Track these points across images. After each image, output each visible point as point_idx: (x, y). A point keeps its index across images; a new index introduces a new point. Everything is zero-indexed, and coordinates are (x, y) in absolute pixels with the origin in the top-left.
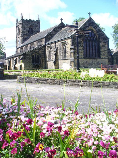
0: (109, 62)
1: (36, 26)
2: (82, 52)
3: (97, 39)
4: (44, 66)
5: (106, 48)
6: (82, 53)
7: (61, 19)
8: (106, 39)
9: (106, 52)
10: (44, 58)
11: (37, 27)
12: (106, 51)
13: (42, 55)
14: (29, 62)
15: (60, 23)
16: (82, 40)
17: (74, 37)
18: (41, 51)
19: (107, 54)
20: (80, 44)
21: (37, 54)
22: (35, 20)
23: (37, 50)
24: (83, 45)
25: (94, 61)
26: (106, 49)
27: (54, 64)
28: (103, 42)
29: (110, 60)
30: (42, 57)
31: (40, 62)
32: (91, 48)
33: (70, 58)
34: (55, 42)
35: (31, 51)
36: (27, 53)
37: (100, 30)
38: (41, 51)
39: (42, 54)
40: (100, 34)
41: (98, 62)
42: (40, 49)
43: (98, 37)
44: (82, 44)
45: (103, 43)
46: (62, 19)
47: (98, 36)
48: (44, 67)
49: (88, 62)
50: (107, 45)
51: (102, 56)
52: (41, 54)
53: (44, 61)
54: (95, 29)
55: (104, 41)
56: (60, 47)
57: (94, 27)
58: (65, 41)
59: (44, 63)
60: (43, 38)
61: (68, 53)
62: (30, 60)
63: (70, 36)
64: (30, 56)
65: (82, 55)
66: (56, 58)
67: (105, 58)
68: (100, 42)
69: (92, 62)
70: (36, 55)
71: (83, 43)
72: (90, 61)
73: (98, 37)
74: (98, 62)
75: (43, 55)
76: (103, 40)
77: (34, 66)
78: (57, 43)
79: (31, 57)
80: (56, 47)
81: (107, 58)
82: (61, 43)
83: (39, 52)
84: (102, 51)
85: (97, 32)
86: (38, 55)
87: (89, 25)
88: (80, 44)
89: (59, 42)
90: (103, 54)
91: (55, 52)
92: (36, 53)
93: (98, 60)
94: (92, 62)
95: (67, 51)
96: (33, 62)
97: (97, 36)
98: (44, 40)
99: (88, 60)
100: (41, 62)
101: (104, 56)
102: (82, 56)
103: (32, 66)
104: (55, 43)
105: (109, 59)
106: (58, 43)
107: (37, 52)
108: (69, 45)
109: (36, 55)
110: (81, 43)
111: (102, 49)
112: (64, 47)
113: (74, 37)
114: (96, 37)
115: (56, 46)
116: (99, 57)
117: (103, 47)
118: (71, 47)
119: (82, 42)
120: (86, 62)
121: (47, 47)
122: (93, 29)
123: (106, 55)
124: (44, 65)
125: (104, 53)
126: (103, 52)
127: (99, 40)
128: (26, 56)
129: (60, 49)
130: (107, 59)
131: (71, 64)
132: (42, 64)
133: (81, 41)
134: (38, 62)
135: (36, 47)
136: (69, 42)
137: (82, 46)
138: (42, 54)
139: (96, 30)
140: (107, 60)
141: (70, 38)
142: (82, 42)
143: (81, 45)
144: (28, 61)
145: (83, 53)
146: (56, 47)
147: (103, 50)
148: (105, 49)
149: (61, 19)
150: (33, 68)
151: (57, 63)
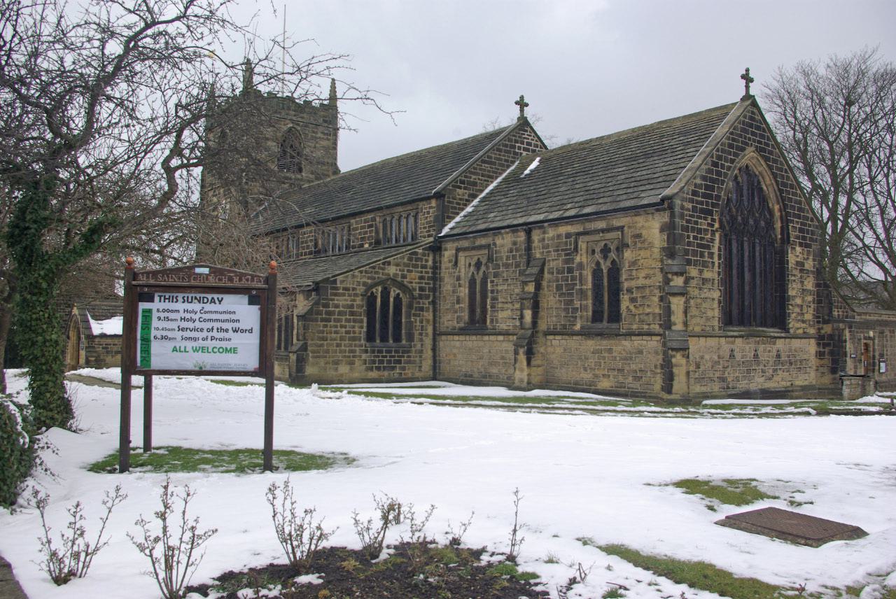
0: (820, 355)
1: (319, 135)
2: (716, 294)
3: (770, 224)
4: (430, 362)
5: (811, 276)
6: (716, 305)
7: (522, 104)
8: (810, 226)
9: (810, 298)
10: (429, 315)
11: (325, 143)
12: (810, 292)
13: (421, 297)
14: (347, 332)
15: (507, 118)
16: (717, 225)
17: (682, 207)
18: (415, 275)
19: (811, 311)
20: (708, 247)
21: (394, 292)
22: (316, 103)
23: (397, 265)
24: (719, 259)
25: (761, 347)
26: (810, 284)
27: (522, 358)
28: (801, 245)
29: (828, 345)
30: (422, 309)
31: (410, 338)
32: (747, 276)
33: (656, 328)
34: (528, 228)
35: (366, 272)
36: (342, 282)
37: (788, 178)
38: (415, 275)
39: (422, 289)
40: (790, 200)
41: (778, 356)
42: (410, 259)
43: (777, 214)
44: (715, 250)
45: (798, 249)
46: (527, 105)
47: (780, 210)
48: (427, 365)
49: (738, 356)
50: (814, 260)
51: (793, 324)
52: (415, 290)
53: (430, 329)
54: (770, 168)
55: (804, 238)
56: (567, 262)
57: (766, 159)
58: (616, 223)
59: (428, 342)
60: (428, 198)
61: (633, 300)
62: (355, 321)
63: (663, 200)
64: (359, 301)
65: (716, 314)
66: (535, 323)
67: (805, 336)
68: (786, 239)
69: (756, 356)
70: (386, 294)
71: (720, 243)
73: (777, 214)
74: (778, 356)
75: (427, 297)
77: (374, 362)
78: (536, 236)
79: (359, 306)
80: (529, 259)
81: (812, 331)
82: (579, 234)
83: (404, 277)
84: (794, 294)
85: (777, 182)
86: (398, 299)
87: (747, 144)
88: (708, 247)
89: (563, 230)
90: (797, 310)
91: (531, 288)
92: (386, 285)
93: (780, 344)
94: (756, 356)
95: (626, 285)
96: (370, 337)
97: (776, 207)
98: (429, 210)
99: (739, 341)
100: (416, 337)
101: (803, 322)
102: (716, 323)
103: (364, 356)
104: (529, 233)
105: (821, 339)
106: (551, 233)
107: (396, 275)
108: (648, 253)
109: (386, 294)
110: (712, 240)
112: (598, 264)
113: (682, 207)
114: (771, 213)
115: (529, 249)
116: (781, 322)
118: (670, 262)
119: (717, 235)
120: (732, 356)
121: (458, 250)
122: (760, 168)
123: (809, 317)
124: (430, 353)
125: (802, 306)
126: (798, 301)
127: (785, 229)
128: (336, 295)
129: (570, 270)
130: (813, 341)
131: (675, 370)
132: (421, 351)
133: (713, 233)
134: (397, 339)
135: (362, 246)
136: (652, 228)
137: (716, 264)
138: (422, 289)
139: (775, 176)
140: (811, 347)
141: (664, 210)
142: (717, 235)
143: (711, 255)
144: (344, 329)
145: (720, 302)
146: (529, 259)
147: (799, 286)
148: (806, 283)
149: (522, 104)
150: (371, 369)
151: (542, 350)
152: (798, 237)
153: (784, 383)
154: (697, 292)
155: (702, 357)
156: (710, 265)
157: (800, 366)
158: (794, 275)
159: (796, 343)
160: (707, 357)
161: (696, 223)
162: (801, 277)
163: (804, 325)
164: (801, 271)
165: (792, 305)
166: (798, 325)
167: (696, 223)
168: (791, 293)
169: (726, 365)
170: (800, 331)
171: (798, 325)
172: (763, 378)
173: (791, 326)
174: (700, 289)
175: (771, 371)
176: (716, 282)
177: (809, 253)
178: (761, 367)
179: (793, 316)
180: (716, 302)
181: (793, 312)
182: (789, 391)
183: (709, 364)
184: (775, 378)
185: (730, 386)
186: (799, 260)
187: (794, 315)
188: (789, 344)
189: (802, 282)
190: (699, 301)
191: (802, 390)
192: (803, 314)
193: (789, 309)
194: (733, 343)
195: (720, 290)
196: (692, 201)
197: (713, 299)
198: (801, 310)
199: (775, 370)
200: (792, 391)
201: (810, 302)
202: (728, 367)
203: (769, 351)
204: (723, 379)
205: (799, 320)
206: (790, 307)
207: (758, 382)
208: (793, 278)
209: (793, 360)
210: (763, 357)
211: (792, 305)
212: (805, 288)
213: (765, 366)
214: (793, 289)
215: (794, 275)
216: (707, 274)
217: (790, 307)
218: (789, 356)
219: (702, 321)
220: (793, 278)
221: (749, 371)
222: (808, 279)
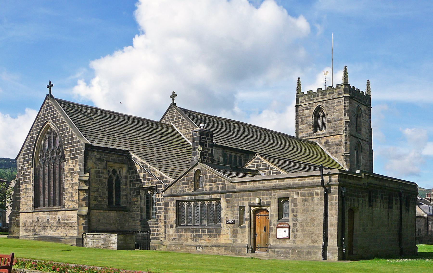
28: (72, 159)
41: (59, 220)
45: (70, 162)
49: (40, 220)
50: (79, 165)
51: (67, 203)
65: (32, 203)
69: (48, 220)
72: (44, 216)
74: (59, 220)
76: (72, 151)
88: (29, 175)
90: (69, 195)
93: (60, 214)
94: (48, 220)
101: (73, 201)
102: (31, 207)
111: (68, 182)
116: (60, 204)
117: (70, 175)
120: (38, 220)
125: (72, 193)
126: (70, 190)
137: (31, 181)
143: (30, 178)
147: (71, 182)
148: (74, 179)
152: (70, 155)
153: (62, 234)
154: (25, 194)
155: (27, 221)
156: (29, 182)
157: (66, 224)
158: (68, 177)
159: (68, 213)
160: (28, 221)
161: (24, 166)
162: (72, 177)
163: (74, 203)
164: (72, 173)
165: (66, 193)
166: (70, 204)
167: (24, 166)
168: (66, 187)
169: (35, 224)
170: (71, 207)
171: (70, 204)
172: (51, 231)
173: (66, 204)
174: (26, 193)
175: (55, 228)
176: (31, 189)
177: (76, 161)
178: (50, 225)
179: (67, 199)
180: (31, 197)
181: (67, 196)
182: (62, 238)
183: (29, 224)
184: (57, 231)
185: (37, 233)
186: (70, 168)
187: (67, 198)
188: (65, 214)
189: (72, 180)
190: (25, 198)
191: (70, 239)
192: (73, 197)
193: (64, 196)
194: (38, 215)
195: (33, 192)
196: (23, 158)
197: (30, 197)
198: (72, 195)
199: (57, 227)
200: (64, 238)
201: (76, 190)
202: (36, 225)
203: (54, 218)
204: (34, 230)
205: (70, 201)
206: (65, 194)
207: (49, 233)
208: (67, 178)
209: (67, 222)
210: (51, 221)
211: (66, 193)
212: (74, 182)
213: (52, 225)
214: (67, 184)
215: (68, 177)
216: (28, 187)
217: (65, 194)
218: (65, 221)
219: (26, 206)
220: (67, 178)
221: (44, 227)
222: (76, 177)
